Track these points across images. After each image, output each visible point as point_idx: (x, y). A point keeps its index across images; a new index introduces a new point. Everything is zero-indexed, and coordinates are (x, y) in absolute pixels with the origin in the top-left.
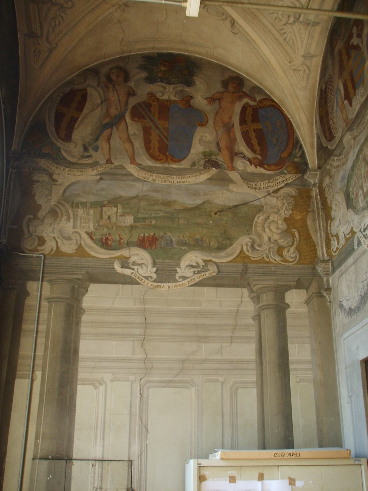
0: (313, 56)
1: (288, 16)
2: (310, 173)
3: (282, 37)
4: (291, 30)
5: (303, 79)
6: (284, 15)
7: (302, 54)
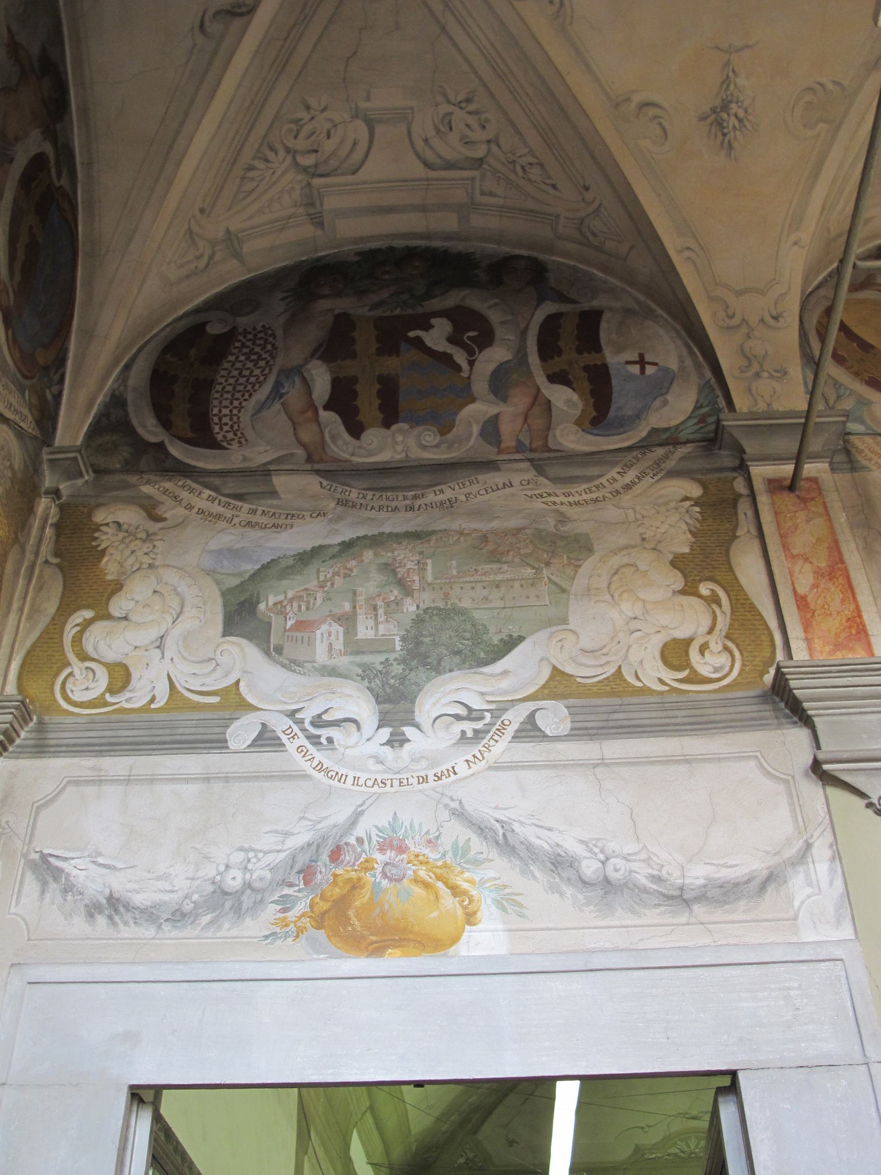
0: (237, 255)
1: (315, 148)
2: (76, 458)
3: (254, 158)
4: (279, 173)
5: (181, 266)
6: (313, 138)
7: (232, 229)
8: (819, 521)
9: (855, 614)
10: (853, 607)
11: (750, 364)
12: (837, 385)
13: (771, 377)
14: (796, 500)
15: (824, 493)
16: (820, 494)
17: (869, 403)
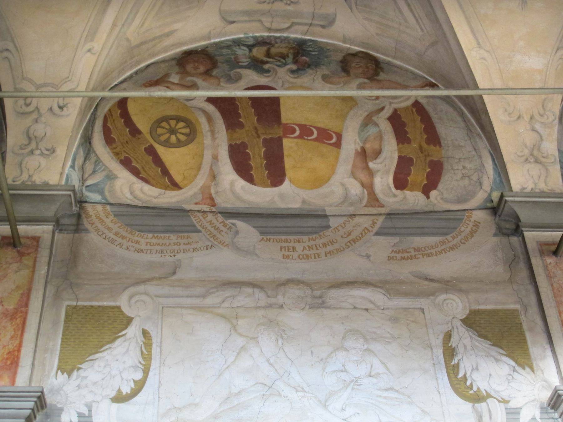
8: (25, 273)
9: (16, 349)
10: (17, 342)
11: (29, 143)
12: (98, 161)
13: (42, 154)
14: (16, 254)
15: (39, 249)
16: (36, 250)
17: (116, 177)
